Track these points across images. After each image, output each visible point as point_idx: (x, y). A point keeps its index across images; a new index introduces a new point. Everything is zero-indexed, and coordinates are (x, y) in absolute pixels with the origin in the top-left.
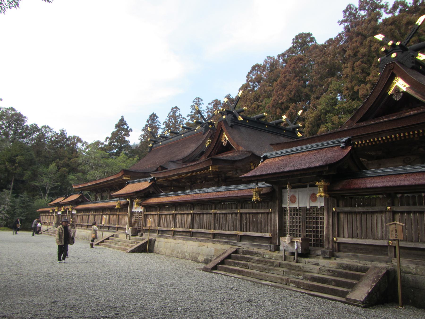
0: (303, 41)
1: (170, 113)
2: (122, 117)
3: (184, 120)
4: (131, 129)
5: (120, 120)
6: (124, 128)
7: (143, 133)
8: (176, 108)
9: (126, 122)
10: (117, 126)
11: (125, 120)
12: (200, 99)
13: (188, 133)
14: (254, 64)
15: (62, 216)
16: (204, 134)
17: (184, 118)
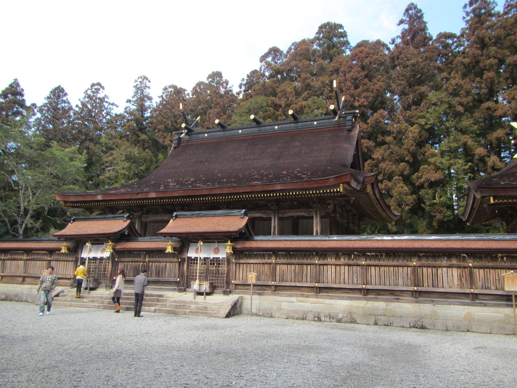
0: (331, 33)
1: (87, 91)
2: (16, 80)
3: (114, 107)
4: (34, 105)
5: (11, 86)
6: (19, 100)
7: (39, 115)
8: (99, 84)
9: (23, 90)
10: (5, 95)
11: (22, 85)
12: (147, 79)
13: (292, 125)
14: (271, 47)
15: (115, 264)
16: (350, 131)
17: (113, 104)
